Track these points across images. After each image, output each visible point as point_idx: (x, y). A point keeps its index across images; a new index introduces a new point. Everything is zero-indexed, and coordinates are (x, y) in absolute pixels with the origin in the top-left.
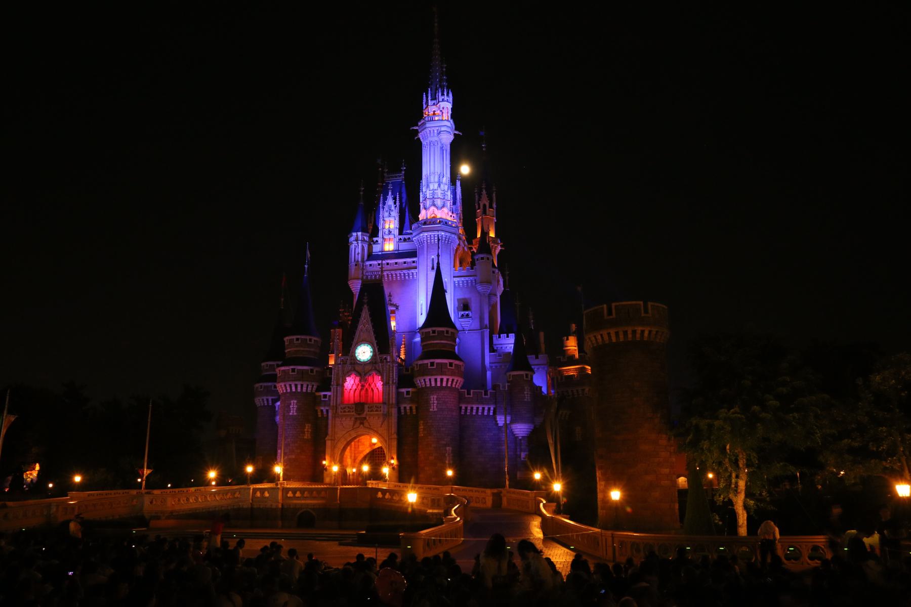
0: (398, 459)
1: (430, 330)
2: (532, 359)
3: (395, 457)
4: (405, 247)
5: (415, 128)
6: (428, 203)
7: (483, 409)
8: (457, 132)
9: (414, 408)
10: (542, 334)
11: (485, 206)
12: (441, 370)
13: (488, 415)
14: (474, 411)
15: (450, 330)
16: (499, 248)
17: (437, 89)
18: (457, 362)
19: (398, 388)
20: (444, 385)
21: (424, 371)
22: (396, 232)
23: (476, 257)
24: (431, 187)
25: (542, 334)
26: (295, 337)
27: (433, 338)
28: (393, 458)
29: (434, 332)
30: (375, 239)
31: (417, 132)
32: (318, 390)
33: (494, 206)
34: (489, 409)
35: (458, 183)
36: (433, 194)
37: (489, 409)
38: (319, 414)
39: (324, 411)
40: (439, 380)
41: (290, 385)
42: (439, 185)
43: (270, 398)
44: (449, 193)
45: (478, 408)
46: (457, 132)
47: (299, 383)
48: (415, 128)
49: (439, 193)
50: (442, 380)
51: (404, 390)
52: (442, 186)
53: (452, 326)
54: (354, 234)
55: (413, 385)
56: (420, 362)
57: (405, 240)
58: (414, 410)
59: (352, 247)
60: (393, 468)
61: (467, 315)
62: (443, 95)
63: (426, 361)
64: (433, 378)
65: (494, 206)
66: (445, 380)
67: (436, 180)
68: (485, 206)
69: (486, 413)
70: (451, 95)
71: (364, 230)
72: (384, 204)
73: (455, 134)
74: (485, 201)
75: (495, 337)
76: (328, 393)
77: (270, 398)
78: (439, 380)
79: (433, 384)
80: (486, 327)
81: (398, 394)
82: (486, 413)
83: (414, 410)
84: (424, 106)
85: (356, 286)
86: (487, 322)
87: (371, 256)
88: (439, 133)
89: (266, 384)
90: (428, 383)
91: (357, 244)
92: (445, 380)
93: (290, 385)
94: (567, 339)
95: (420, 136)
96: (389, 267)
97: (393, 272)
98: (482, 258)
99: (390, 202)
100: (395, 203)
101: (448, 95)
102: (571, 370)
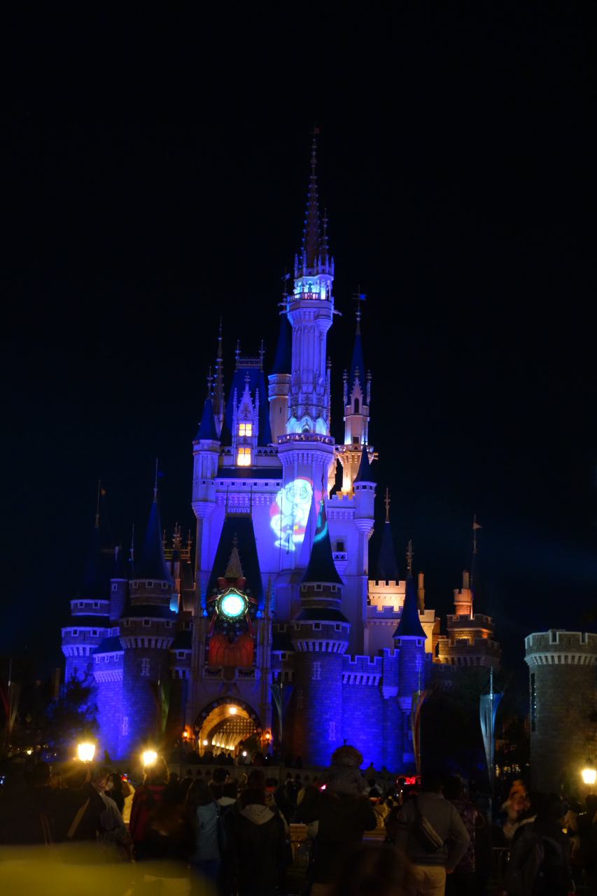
4: (267, 462)
5: (283, 304)
7: (368, 678)
8: (336, 312)
9: (290, 673)
10: (421, 577)
11: (357, 401)
12: (327, 633)
13: (373, 685)
14: (358, 680)
15: (338, 585)
19: (273, 649)
20: (330, 650)
21: (307, 633)
22: (256, 441)
24: (304, 388)
25: (421, 577)
26: (147, 581)
27: (318, 594)
29: (319, 587)
30: (226, 449)
32: (174, 646)
33: (368, 400)
34: (374, 678)
36: (307, 398)
37: (374, 678)
38: (174, 675)
39: (181, 672)
40: (324, 644)
41: (143, 640)
42: (315, 388)
43: (88, 647)
47: (154, 638)
48: (283, 304)
49: (314, 398)
50: (327, 644)
51: (279, 653)
52: (318, 388)
55: (291, 648)
56: (302, 622)
58: (290, 677)
61: (343, 557)
62: (323, 264)
63: (310, 622)
64: (317, 642)
66: (331, 645)
68: (357, 401)
69: (370, 683)
72: (239, 401)
74: (357, 394)
76: (186, 651)
77: (88, 647)
78: (324, 644)
79: (317, 649)
81: (273, 656)
82: (364, 683)
83: (290, 677)
88: (316, 317)
89: (82, 629)
91: (204, 457)
92: (331, 645)
93: (143, 640)
94: (460, 593)
98: (364, 487)
99: (247, 399)
100: (254, 402)
102: (465, 635)
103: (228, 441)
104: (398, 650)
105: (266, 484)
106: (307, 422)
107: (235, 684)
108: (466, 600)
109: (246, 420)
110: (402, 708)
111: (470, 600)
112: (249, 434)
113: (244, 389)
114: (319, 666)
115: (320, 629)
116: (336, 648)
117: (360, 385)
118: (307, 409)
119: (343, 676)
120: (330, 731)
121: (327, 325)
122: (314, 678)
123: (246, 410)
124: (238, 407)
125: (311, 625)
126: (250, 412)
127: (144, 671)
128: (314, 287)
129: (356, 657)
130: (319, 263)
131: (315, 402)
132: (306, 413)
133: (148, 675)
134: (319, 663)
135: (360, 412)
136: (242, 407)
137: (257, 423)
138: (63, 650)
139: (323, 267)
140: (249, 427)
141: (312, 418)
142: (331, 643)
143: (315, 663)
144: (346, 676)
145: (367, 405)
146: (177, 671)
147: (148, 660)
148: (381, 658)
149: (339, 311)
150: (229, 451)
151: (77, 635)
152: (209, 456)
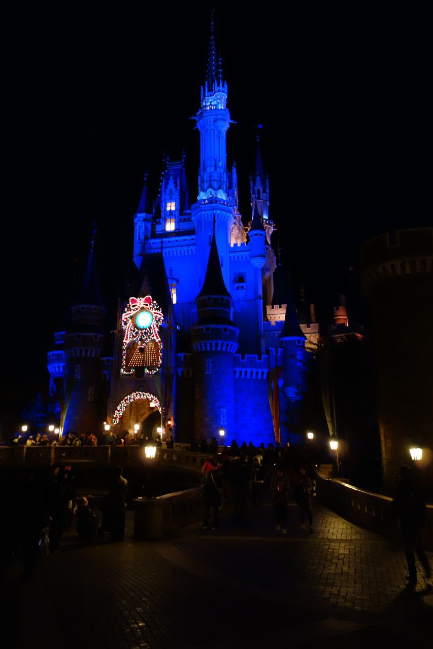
0: (175, 421)
1: (206, 297)
2: (303, 327)
3: (172, 418)
4: (185, 226)
5: (193, 118)
6: (206, 185)
7: (257, 373)
8: (232, 122)
10: (312, 306)
13: (262, 379)
14: (248, 375)
16: (272, 229)
17: (213, 81)
18: (231, 328)
22: (177, 213)
23: (221, 90)
24: (208, 170)
25: (312, 306)
28: (170, 420)
29: (209, 299)
30: (158, 221)
31: (195, 122)
34: (263, 373)
35: (234, 170)
36: (210, 177)
37: (263, 373)
40: (214, 344)
42: (216, 169)
44: (225, 176)
45: (252, 372)
46: (232, 122)
48: (193, 118)
49: (215, 175)
51: (182, 355)
52: (218, 169)
53: (228, 295)
54: (139, 215)
57: (185, 220)
59: (137, 227)
60: (170, 429)
61: (242, 287)
62: (218, 85)
63: (201, 327)
65: (267, 191)
67: (213, 164)
68: (259, 191)
70: (226, 86)
71: (148, 211)
72: (166, 188)
73: (230, 123)
75: (268, 308)
76: (111, 358)
78: (214, 344)
80: (260, 298)
84: (202, 98)
85: (137, 261)
86: (260, 293)
87: (154, 235)
88: (215, 121)
89: (57, 352)
90: (204, 348)
91: (140, 222)
94: (338, 309)
95: (198, 125)
96: (169, 244)
97: (174, 249)
99: (171, 186)
100: (176, 187)
101: (223, 86)
103: (158, 216)
104: (282, 349)
105: (184, 240)
106: (211, 193)
107: (145, 381)
108: (343, 314)
109: (171, 200)
110: (288, 396)
111: (345, 314)
112: (173, 208)
113: (169, 180)
114: (210, 363)
115: (210, 332)
116: (229, 348)
117: (260, 180)
118: (210, 183)
119: (235, 372)
120: (221, 416)
121: (225, 126)
122: (206, 373)
123: (171, 191)
124: (165, 192)
125: (203, 329)
126: (173, 194)
127: (76, 375)
128: (216, 101)
129: (246, 355)
130: (216, 85)
131: (216, 178)
132: (211, 186)
133: (79, 377)
134: (210, 360)
135: (261, 198)
136: (168, 192)
137: (178, 201)
138: (48, 369)
139: (219, 88)
140: (173, 204)
141: (214, 189)
142: (220, 343)
143: (207, 360)
144: (238, 371)
145: (267, 194)
146: (105, 375)
147: (80, 366)
148: (267, 356)
149: (234, 121)
150: (160, 222)
151: (54, 357)
152: (143, 224)
